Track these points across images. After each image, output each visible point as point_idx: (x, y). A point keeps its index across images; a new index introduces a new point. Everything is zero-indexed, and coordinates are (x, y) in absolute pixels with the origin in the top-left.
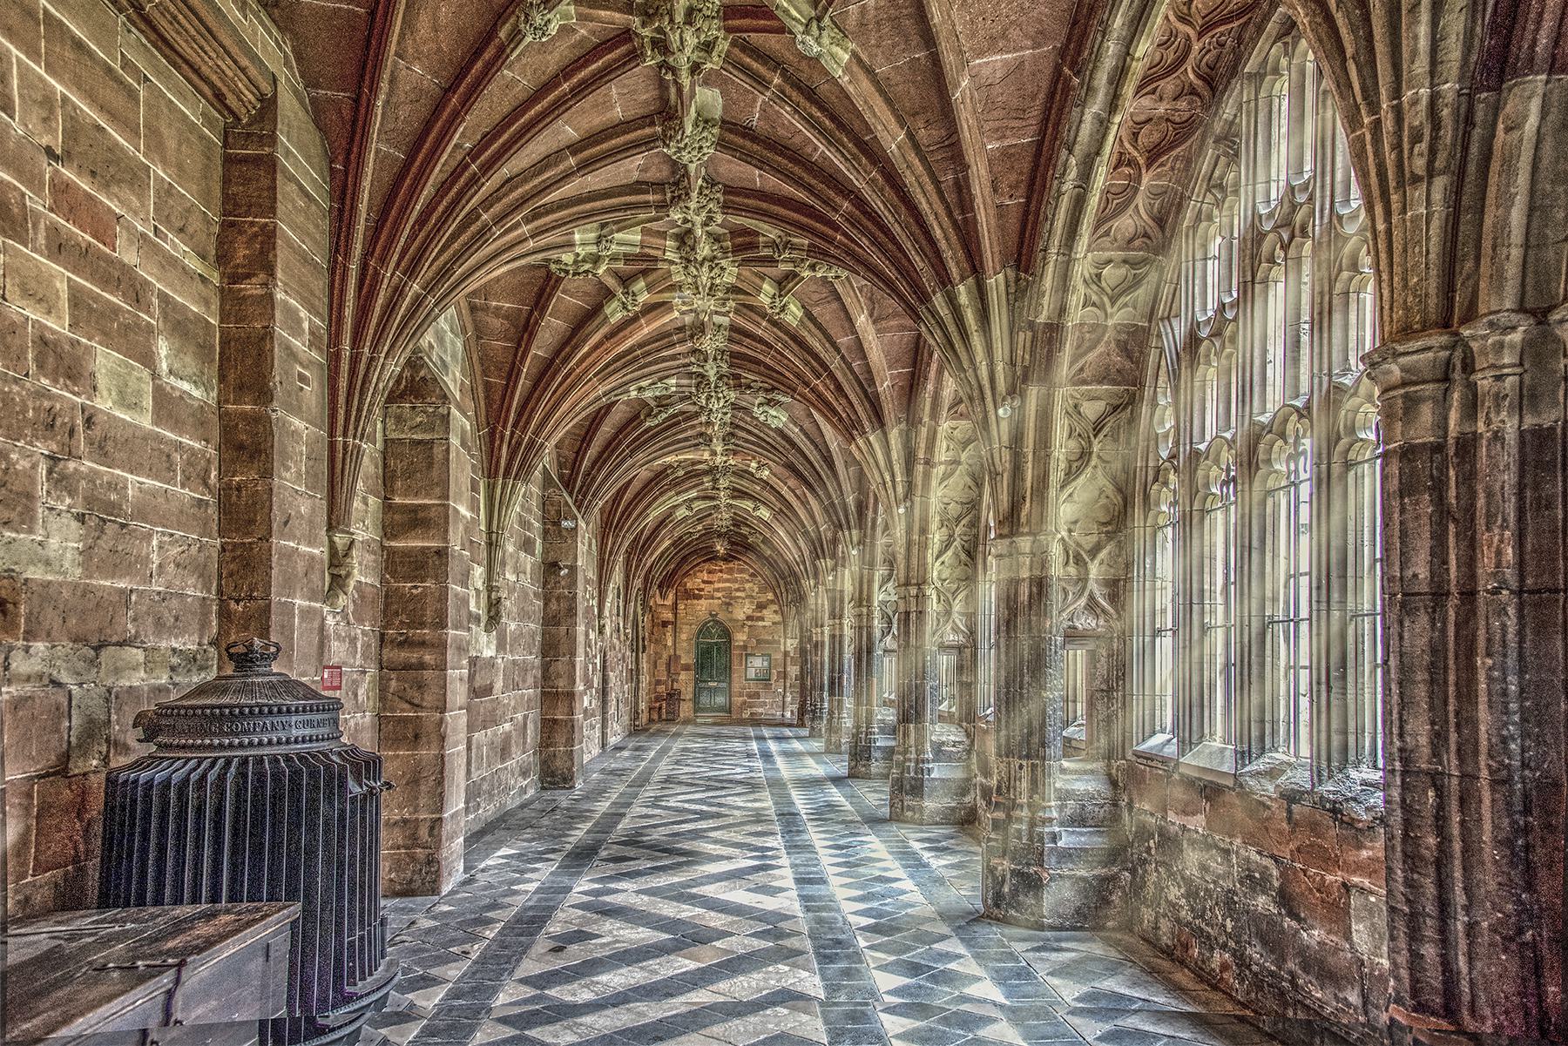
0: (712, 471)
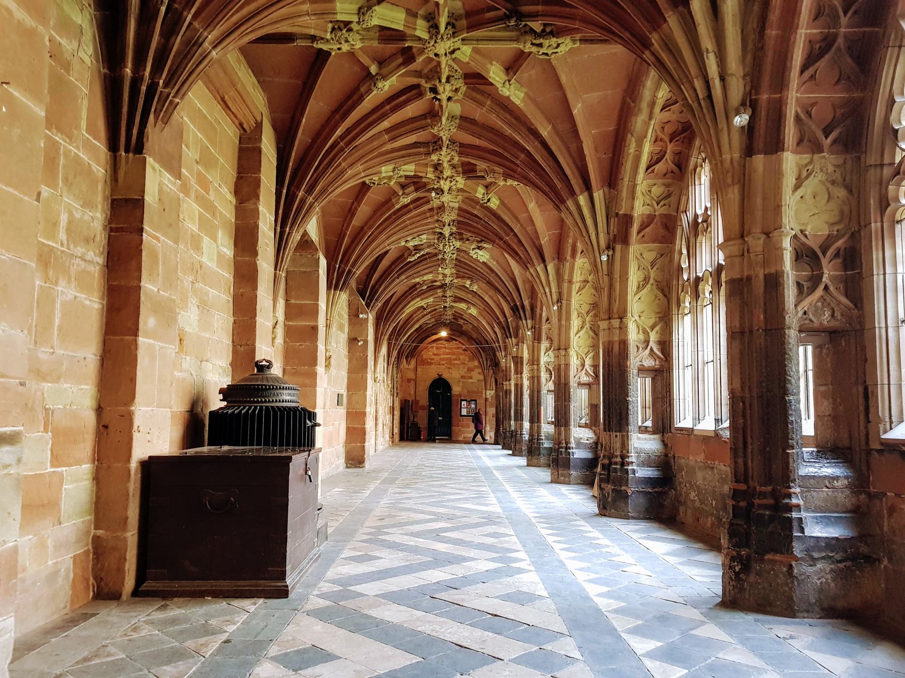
0: (443, 286)
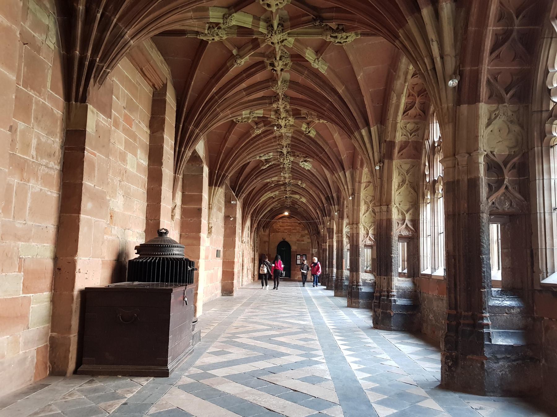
0: (285, 184)
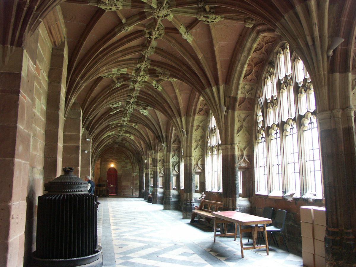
0: (122, 126)
